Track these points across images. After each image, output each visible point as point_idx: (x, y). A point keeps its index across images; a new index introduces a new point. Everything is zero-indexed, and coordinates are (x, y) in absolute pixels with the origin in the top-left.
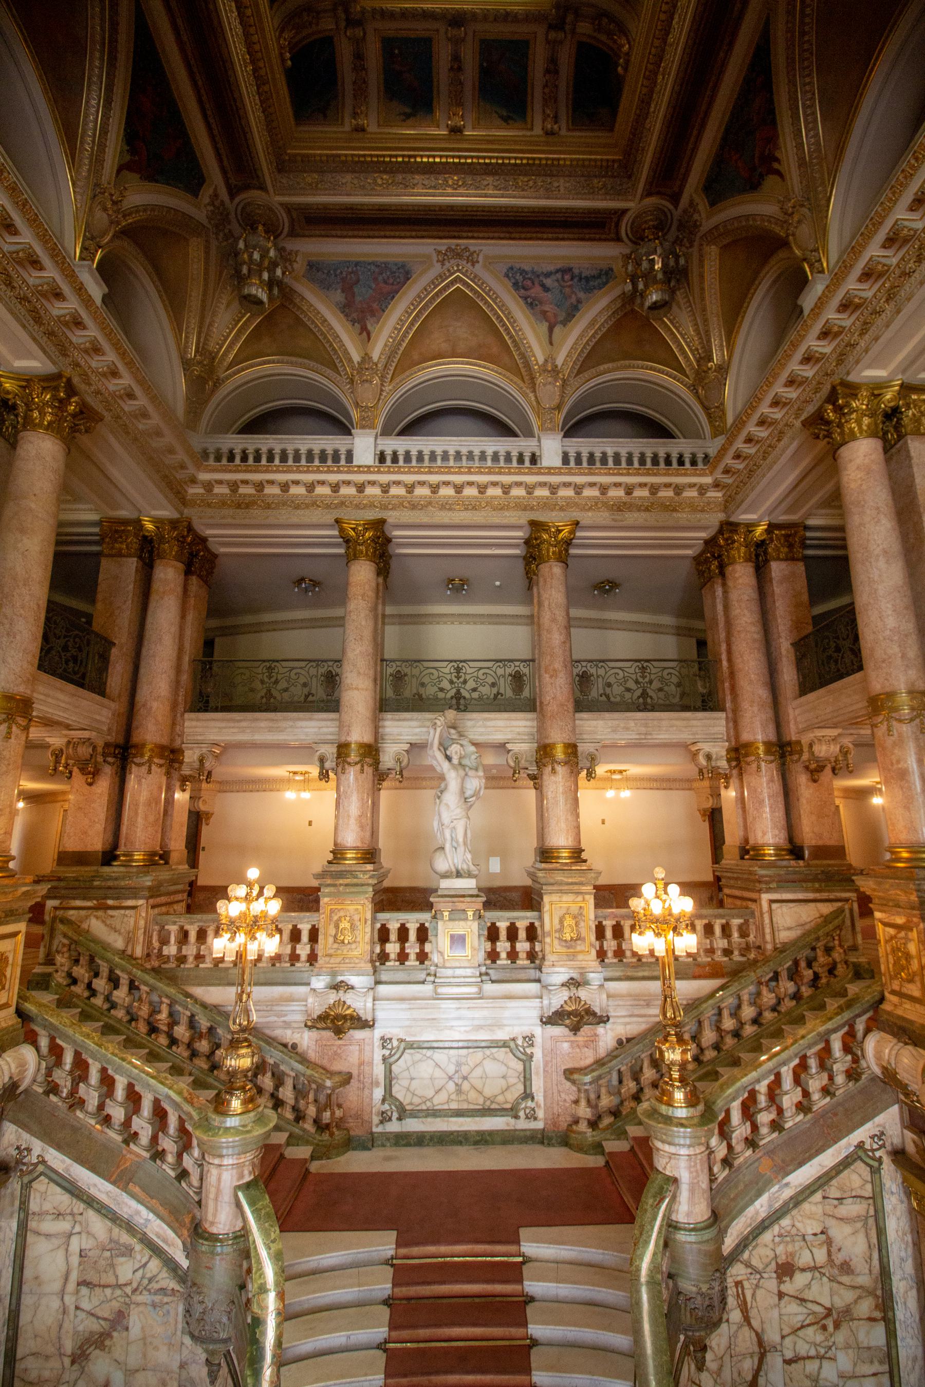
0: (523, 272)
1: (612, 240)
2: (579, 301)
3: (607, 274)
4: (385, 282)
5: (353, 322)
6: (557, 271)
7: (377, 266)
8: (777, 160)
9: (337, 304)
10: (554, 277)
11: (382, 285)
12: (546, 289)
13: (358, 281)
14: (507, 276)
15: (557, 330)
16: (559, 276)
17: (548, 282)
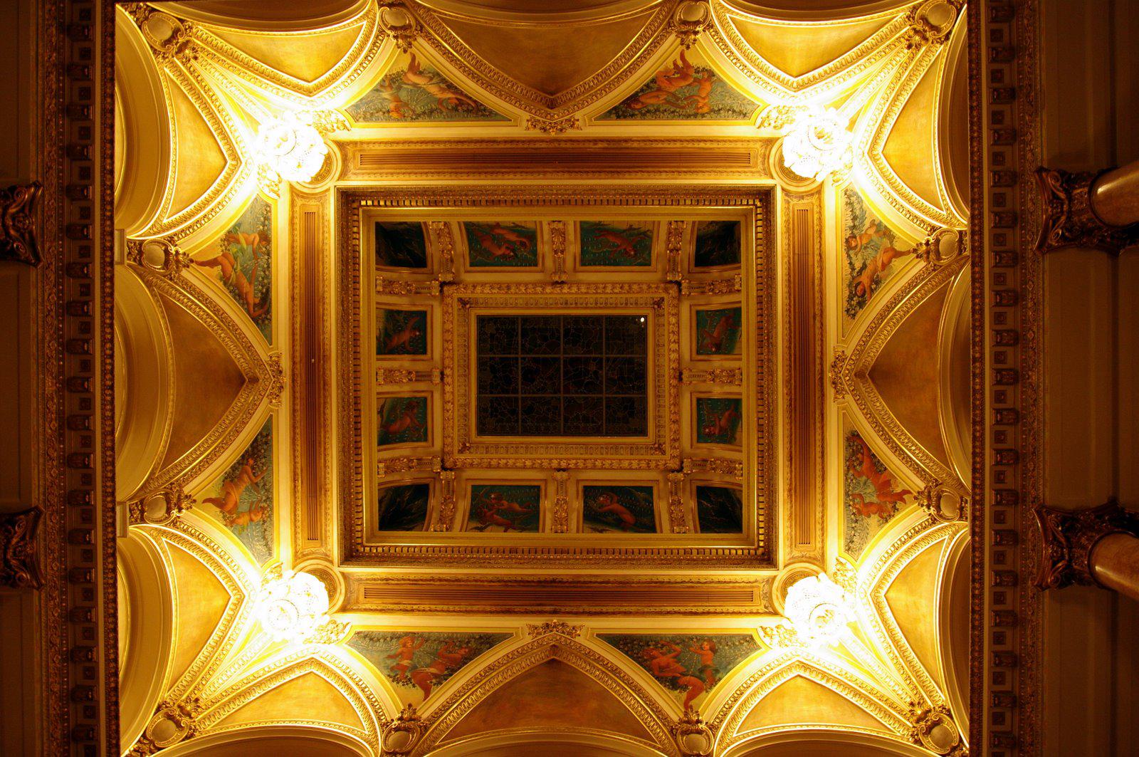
0: (851, 298)
1: (820, 199)
2: (873, 223)
3: (849, 197)
4: (860, 464)
5: (895, 509)
6: (849, 256)
7: (848, 471)
8: (675, 64)
9: (880, 526)
10: (854, 258)
11: (865, 465)
12: (864, 267)
13: (860, 496)
14: (854, 315)
15: (898, 247)
16: (852, 253)
17: (858, 265)
